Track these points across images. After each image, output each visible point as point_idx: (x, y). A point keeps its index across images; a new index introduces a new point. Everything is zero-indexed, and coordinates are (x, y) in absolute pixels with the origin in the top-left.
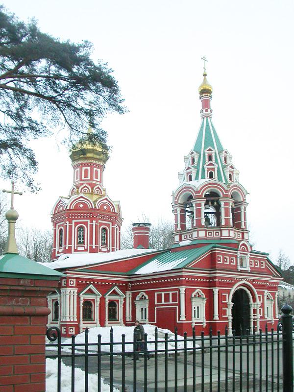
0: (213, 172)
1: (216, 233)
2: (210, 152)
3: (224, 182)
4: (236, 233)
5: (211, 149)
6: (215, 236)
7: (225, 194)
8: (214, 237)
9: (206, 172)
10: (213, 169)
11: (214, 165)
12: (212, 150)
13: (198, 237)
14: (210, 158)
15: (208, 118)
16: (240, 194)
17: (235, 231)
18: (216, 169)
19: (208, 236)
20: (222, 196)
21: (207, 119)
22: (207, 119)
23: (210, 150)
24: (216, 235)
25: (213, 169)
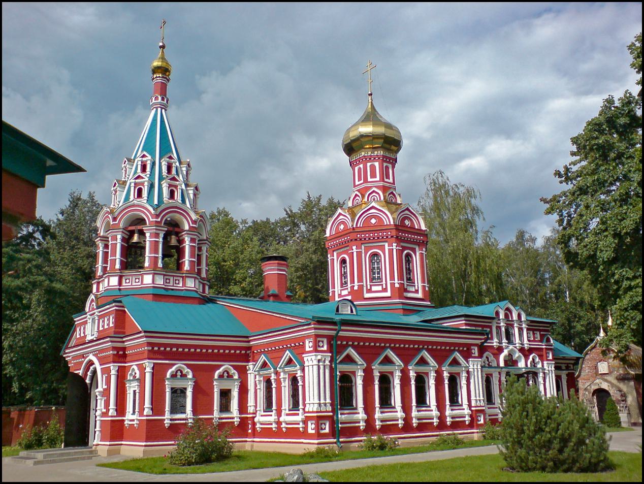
0: (142, 187)
1: (136, 279)
2: (144, 159)
3: (156, 202)
4: (172, 278)
5: (147, 155)
6: (134, 284)
7: (151, 220)
8: (132, 285)
9: (132, 189)
10: (143, 184)
11: (143, 178)
12: (147, 157)
13: (108, 286)
14: (144, 168)
15: (163, 110)
16: (185, 220)
17: (164, 275)
18: (146, 184)
19: (124, 284)
20: (148, 224)
21: (157, 111)
22: (157, 111)
23: (144, 156)
24: (135, 282)
25: (143, 184)
